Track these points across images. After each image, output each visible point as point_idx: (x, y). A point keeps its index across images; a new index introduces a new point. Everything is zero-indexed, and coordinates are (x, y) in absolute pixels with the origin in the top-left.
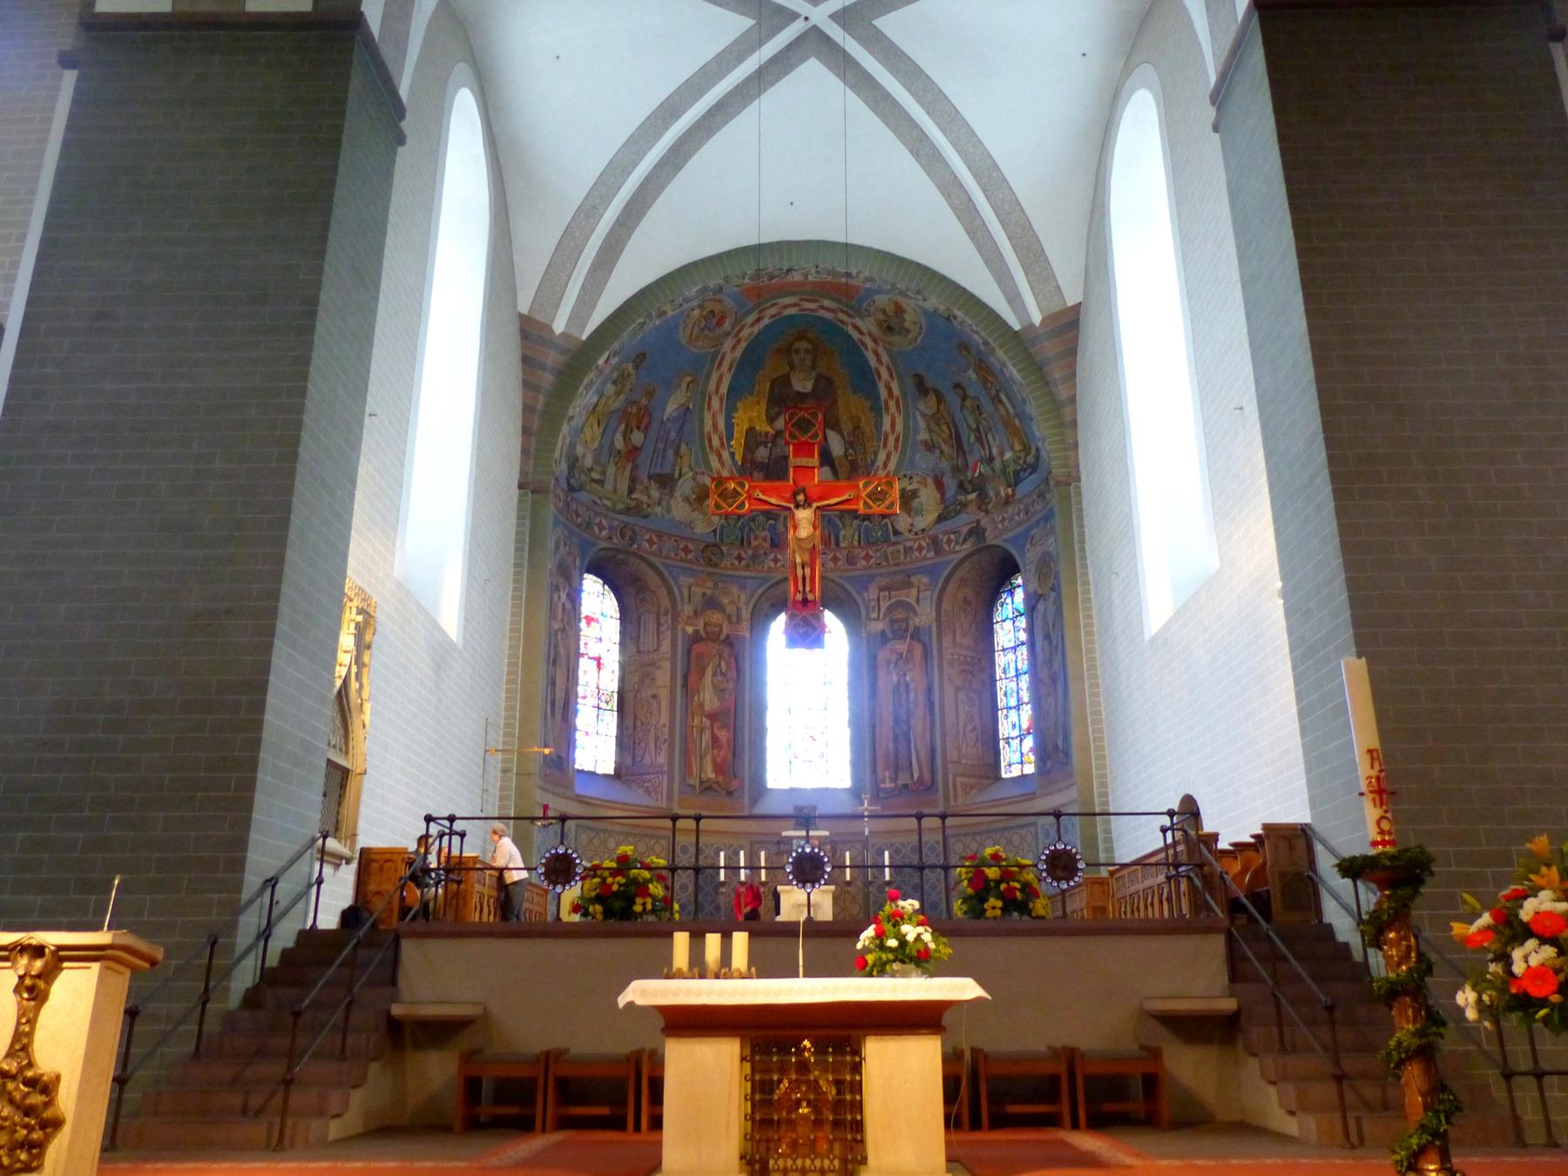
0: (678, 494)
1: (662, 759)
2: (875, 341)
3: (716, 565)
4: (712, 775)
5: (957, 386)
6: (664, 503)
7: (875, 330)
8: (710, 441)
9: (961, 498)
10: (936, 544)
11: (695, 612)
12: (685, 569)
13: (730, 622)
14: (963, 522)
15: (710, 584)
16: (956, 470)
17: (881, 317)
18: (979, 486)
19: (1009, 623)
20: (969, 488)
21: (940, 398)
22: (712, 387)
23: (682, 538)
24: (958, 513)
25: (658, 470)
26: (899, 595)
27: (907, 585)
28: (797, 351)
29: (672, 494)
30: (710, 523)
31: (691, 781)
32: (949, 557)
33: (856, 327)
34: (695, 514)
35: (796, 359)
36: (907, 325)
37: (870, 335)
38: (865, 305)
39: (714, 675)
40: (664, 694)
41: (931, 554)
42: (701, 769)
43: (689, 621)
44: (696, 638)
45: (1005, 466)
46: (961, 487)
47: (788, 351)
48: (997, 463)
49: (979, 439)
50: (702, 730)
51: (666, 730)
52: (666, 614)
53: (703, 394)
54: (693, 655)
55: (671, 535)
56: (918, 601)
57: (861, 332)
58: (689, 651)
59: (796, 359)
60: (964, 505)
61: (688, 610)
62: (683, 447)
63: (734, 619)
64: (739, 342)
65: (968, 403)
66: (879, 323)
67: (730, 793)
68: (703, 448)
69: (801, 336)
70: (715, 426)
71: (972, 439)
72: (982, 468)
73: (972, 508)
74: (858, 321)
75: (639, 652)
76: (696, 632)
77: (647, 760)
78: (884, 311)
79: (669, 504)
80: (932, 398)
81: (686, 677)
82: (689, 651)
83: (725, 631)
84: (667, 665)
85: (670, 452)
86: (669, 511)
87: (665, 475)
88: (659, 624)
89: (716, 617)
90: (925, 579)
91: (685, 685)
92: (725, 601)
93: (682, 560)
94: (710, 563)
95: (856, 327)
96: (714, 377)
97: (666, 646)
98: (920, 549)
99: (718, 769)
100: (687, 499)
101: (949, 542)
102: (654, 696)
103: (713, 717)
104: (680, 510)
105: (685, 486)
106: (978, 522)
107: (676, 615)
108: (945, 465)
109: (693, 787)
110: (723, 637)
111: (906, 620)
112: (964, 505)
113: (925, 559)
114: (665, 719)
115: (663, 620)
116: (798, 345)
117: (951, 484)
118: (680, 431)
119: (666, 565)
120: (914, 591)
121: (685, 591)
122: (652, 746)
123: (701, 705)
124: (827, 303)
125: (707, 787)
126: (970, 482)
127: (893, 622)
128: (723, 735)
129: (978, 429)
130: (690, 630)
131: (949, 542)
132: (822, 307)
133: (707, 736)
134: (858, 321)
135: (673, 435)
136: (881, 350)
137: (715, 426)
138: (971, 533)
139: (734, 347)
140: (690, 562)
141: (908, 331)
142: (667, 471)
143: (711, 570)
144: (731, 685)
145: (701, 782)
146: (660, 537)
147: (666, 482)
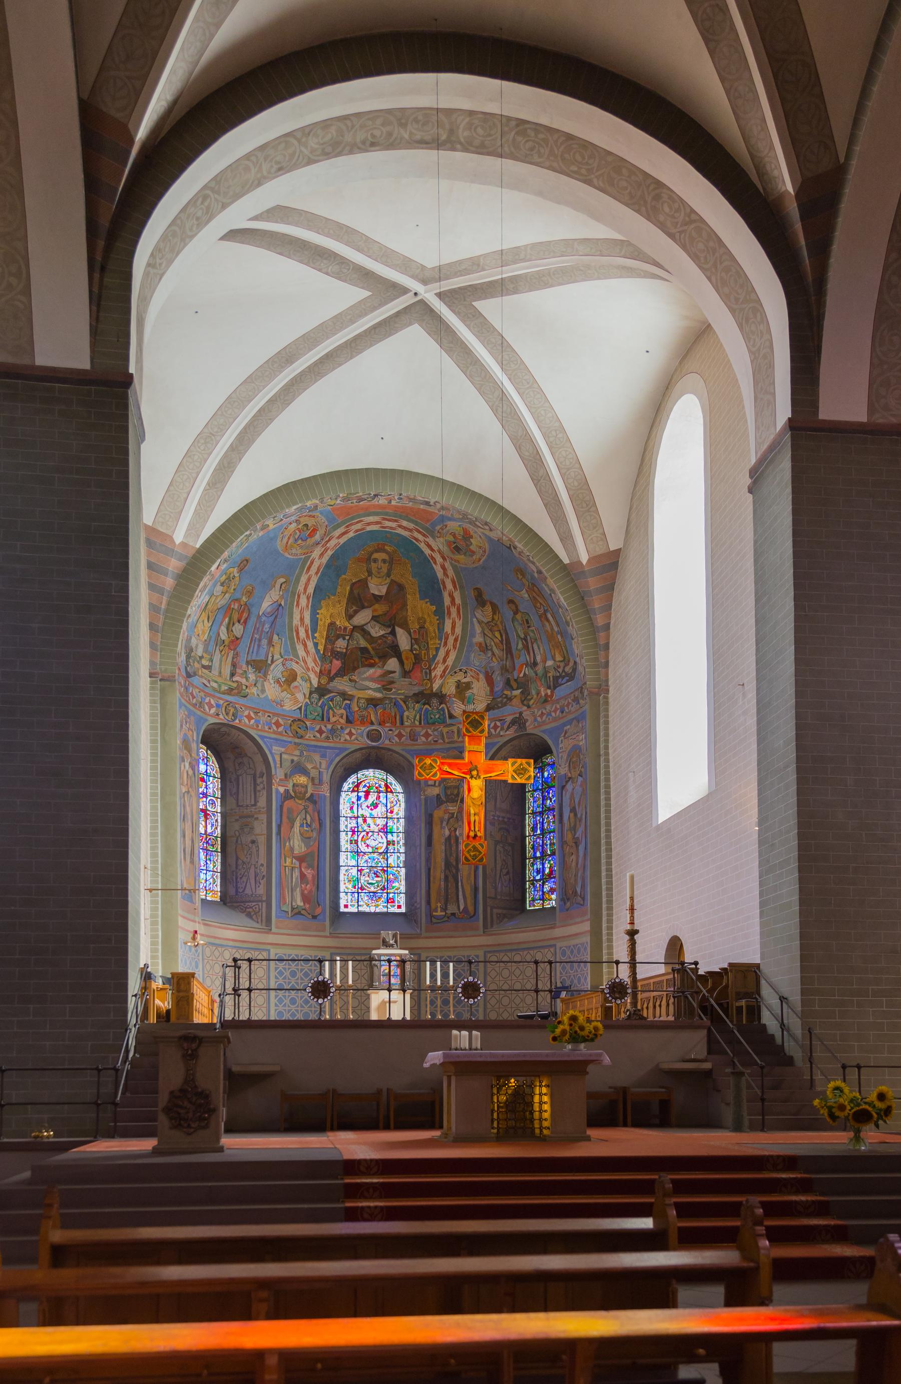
6: (259, 685)
11: (286, 775)
13: (313, 784)
22: (301, 587)
32: (496, 740)
52: (262, 776)
55: (265, 711)
76: (287, 791)
79: (263, 686)
85: (264, 642)
86: (263, 691)
87: (261, 661)
89: (302, 780)
93: (275, 732)
108: (495, 664)
110: (308, 795)
119: (262, 737)
121: (278, 758)
135: (267, 626)
142: (263, 658)
146: (256, 713)
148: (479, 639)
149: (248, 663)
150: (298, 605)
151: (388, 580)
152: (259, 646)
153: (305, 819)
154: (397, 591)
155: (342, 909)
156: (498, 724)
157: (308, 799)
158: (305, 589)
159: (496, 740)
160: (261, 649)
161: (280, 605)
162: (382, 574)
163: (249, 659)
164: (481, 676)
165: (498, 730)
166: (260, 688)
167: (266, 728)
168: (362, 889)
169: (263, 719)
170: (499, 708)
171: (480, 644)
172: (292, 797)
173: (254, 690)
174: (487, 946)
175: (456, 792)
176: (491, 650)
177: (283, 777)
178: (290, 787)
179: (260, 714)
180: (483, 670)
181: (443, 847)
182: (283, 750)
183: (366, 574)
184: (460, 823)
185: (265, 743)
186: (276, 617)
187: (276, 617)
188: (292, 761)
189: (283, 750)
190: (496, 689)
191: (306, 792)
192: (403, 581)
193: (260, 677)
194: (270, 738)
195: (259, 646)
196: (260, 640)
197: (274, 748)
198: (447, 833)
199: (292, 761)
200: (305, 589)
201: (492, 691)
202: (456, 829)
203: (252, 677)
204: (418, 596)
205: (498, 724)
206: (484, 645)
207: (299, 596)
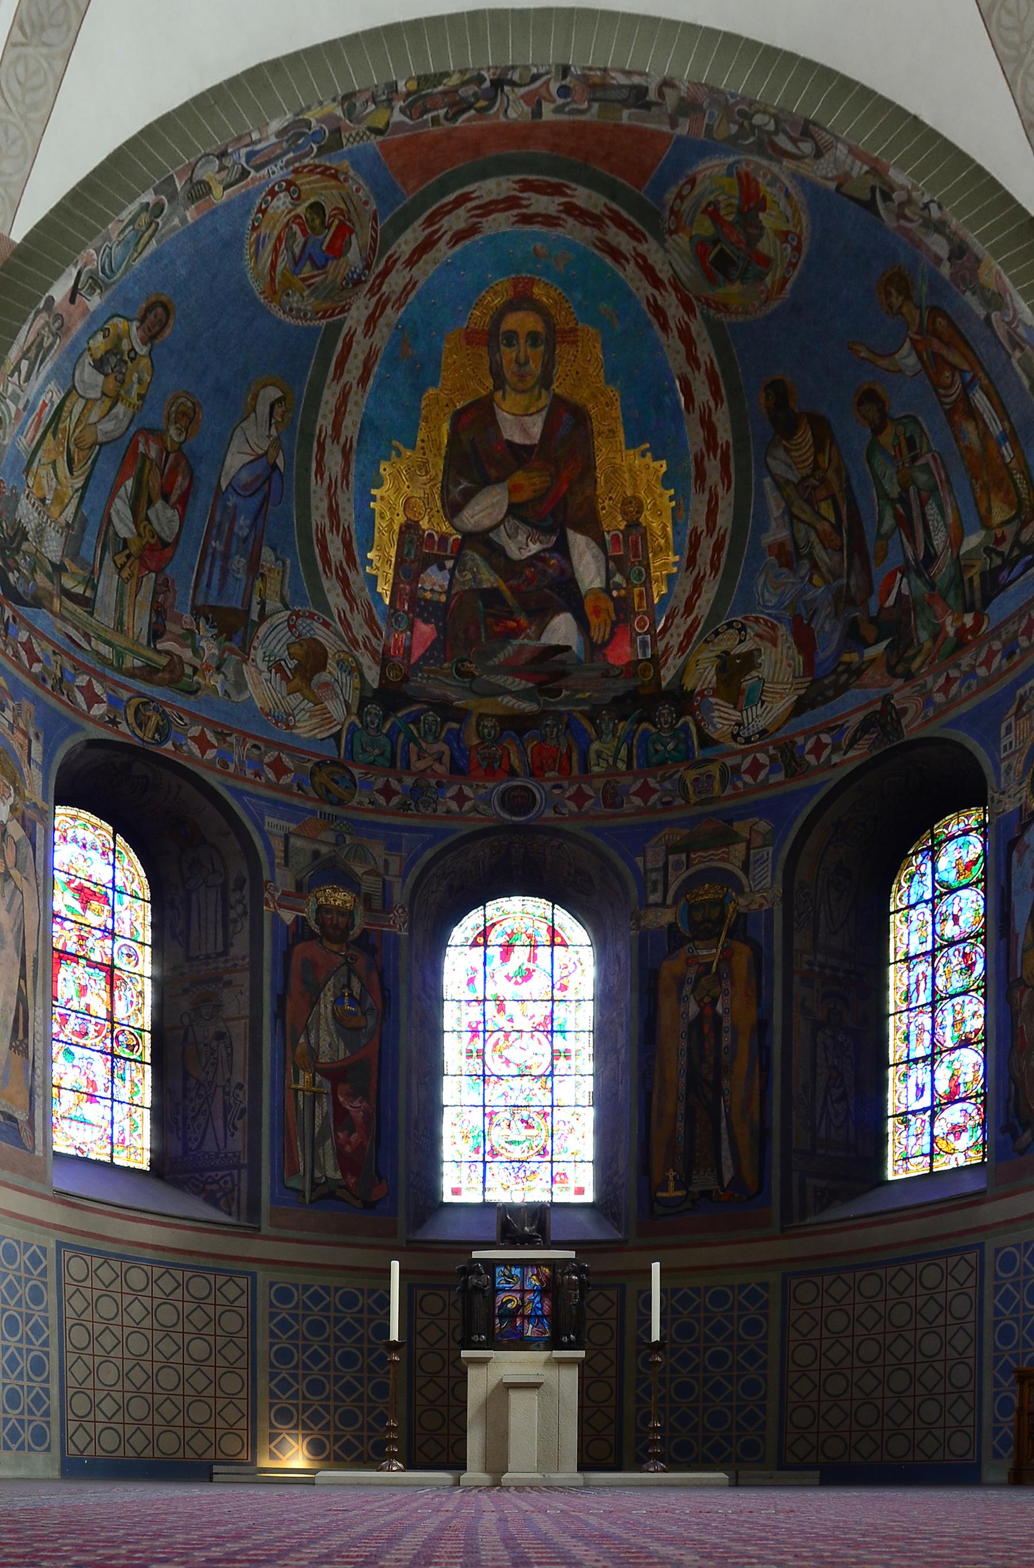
0: (258, 654)
1: (238, 1143)
2: (687, 306)
3: (340, 803)
4: (332, 1172)
5: (869, 396)
6: (229, 670)
7: (687, 270)
8: (324, 549)
9: (854, 657)
10: (789, 758)
11: (299, 885)
12: (276, 803)
14: (852, 707)
15: (329, 836)
16: (843, 600)
17: (705, 227)
18: (896, 627)
19: (925, 910)
20: (869, 632)
21: (822, 431)
22: (324, 421)
23: (271, 744)
24: (840, 689)
25: (212, 602)
26: (703, 860)
27: (727, 838)
28: (511, 338)
29: (245, 649)
30: (327, 719)
31: (293, 1183)
32: (818, 779)
33: (648, 271)
34: (295, 700)
35: (508, 354)
36: (766, 246)
37: (677, 284)
38: (670, 196)
39: (338, 1000)
40: (239, 1029)
41: (780, 777)
42: (315, 1162)
43: (286, 900)
44: (300, 931)
45: (958, 579)
46: (854, 637)
47: (491, 337)
48: (942, 571)
49: (905, 523)
50: (315, 1096)
51: (244, 1098)
53: (307, 435)
54: (296, 962)
55: (246, 735)
56: (746, 867)
57: (656, 282)
58: (287, 955)
59: (508, 354)
60: (857, 672)
61: (283, 880)
62: (267, 554)
63: (377, 904)
64: (382, 305)
65: (886, 438)
66: (701, 247)
67: (369, 1205)
68: (309, 562)
69: (521, 299)
70: (333, 513)
71: (889, 521)
72: (903, 585)
73: (872, 675)
74: (650, 249)
75: (189, 959)
77: (210, 1146)
78: (713, 212)
79: (239, 673)
80: (805, 436)
81: (281, 1000)
82: (287, 955)
83: (359, 921)
84: (243, 979)
85: (239, 563)
86: (240, 685)
87: (233, 611)
88: (226, 906)
89: (341, 898)
90: (763, 826)
91: (279, 1015)
92: (359, 870)
93: (269, 785)
94: (326, 796)
95: (648, 271)
96: (330, 396)
97: (240, 946)
98: (755, 768)
99: (344, 1162)
100: (278, 667)
101: (818, 748)
102: (220, 1036)
103: (336, 1075)
104: (262, 688)
105: (273, 639)
106: (886, 700)
107: (258, 886)
108: (818, 590)
109: (300, 1192)
110: (355, 933)
111: (721, 903)
112: (857, 672)
113: (765, 786)
114: (240, 1075)
115: (234, 897)
116: (512, 322)
117: (828, 630)
118: (259, 514)
120: (740, 849)
121: (278, 845)
122: (219, 1124)
123: (313, 1052)
124: (582, 196)
125: (325, 1194)
126: (873, 620)
127: (692, 908)
128: (356, 1108)
129: (904, 499)
130: (288, 917)
131: (818, 748)
132: (570, 209)
133: (324, 1108)
134: (650, 249)
135: (243, 522)
136: (697, 327)
137: (333, 513)
138: (865, 727)
139: (371, 321)
140: (286, 790)
141: (766, 262)
142: (237, 604)
143: (328, 809)
144: (371, 1022)
145: (315, 1184)
146: (222, 736)
147: (234, 626)
148: (777, 533)
149: (198, 612)
150: (320, 471)
151: (545, 400)
152: (225, 572)
153: (348, 985)
154: (569, 424)
155: (448, 1197)
156: (826, 738)
157: (356, 942)
158: (337, 426)
159: (818, 779)
160: (230, 580)
161: (274, 467)
162: (530, 381)
163: (200, 602)
164: (783, 630)
165: (826, 753)
166: (231, 677)
167: (249, 773)
168: (494, 1153)
169: (240, 751)
170: (827, 700)
171: (781, 545)
172: (313, 936)
173: (216, 681)
174: (792, 1260)
175: (715, 913)
176: (810, 556)
177: (292, 889)
178: (309, 912)
179: (232, 739)
180: (787, 615)
181: (684, 1044)
182: (293, 827)
183: (489, 383)
184: (726, 985)
185: (245, 807)
186: (266, 499)
187: (266, 499)
188: (316, 854)
189: (293, 827)
190: (821, 656)
191: (350, 926)
192: (581, 396)
193: (232, 651)
194: (260, 798)
195: (225, 572)
196: (226, 557)
197: (268, 819)
198: (693, 1009)
199: (316, 854)
200: (337, 426)
201: (809, 665)
202: (715, 1001)
203: (210, 648)
204: (621, 436)
205: (826, 738)
206: (790, 548)
207: (321, 447)
